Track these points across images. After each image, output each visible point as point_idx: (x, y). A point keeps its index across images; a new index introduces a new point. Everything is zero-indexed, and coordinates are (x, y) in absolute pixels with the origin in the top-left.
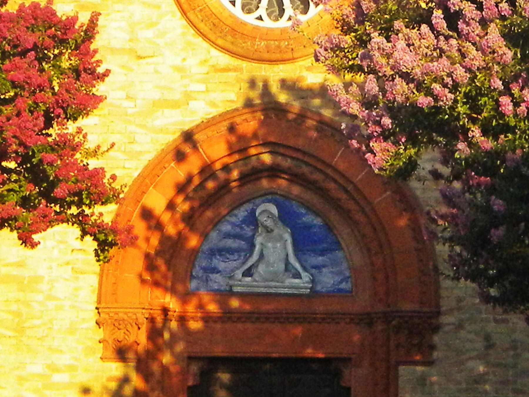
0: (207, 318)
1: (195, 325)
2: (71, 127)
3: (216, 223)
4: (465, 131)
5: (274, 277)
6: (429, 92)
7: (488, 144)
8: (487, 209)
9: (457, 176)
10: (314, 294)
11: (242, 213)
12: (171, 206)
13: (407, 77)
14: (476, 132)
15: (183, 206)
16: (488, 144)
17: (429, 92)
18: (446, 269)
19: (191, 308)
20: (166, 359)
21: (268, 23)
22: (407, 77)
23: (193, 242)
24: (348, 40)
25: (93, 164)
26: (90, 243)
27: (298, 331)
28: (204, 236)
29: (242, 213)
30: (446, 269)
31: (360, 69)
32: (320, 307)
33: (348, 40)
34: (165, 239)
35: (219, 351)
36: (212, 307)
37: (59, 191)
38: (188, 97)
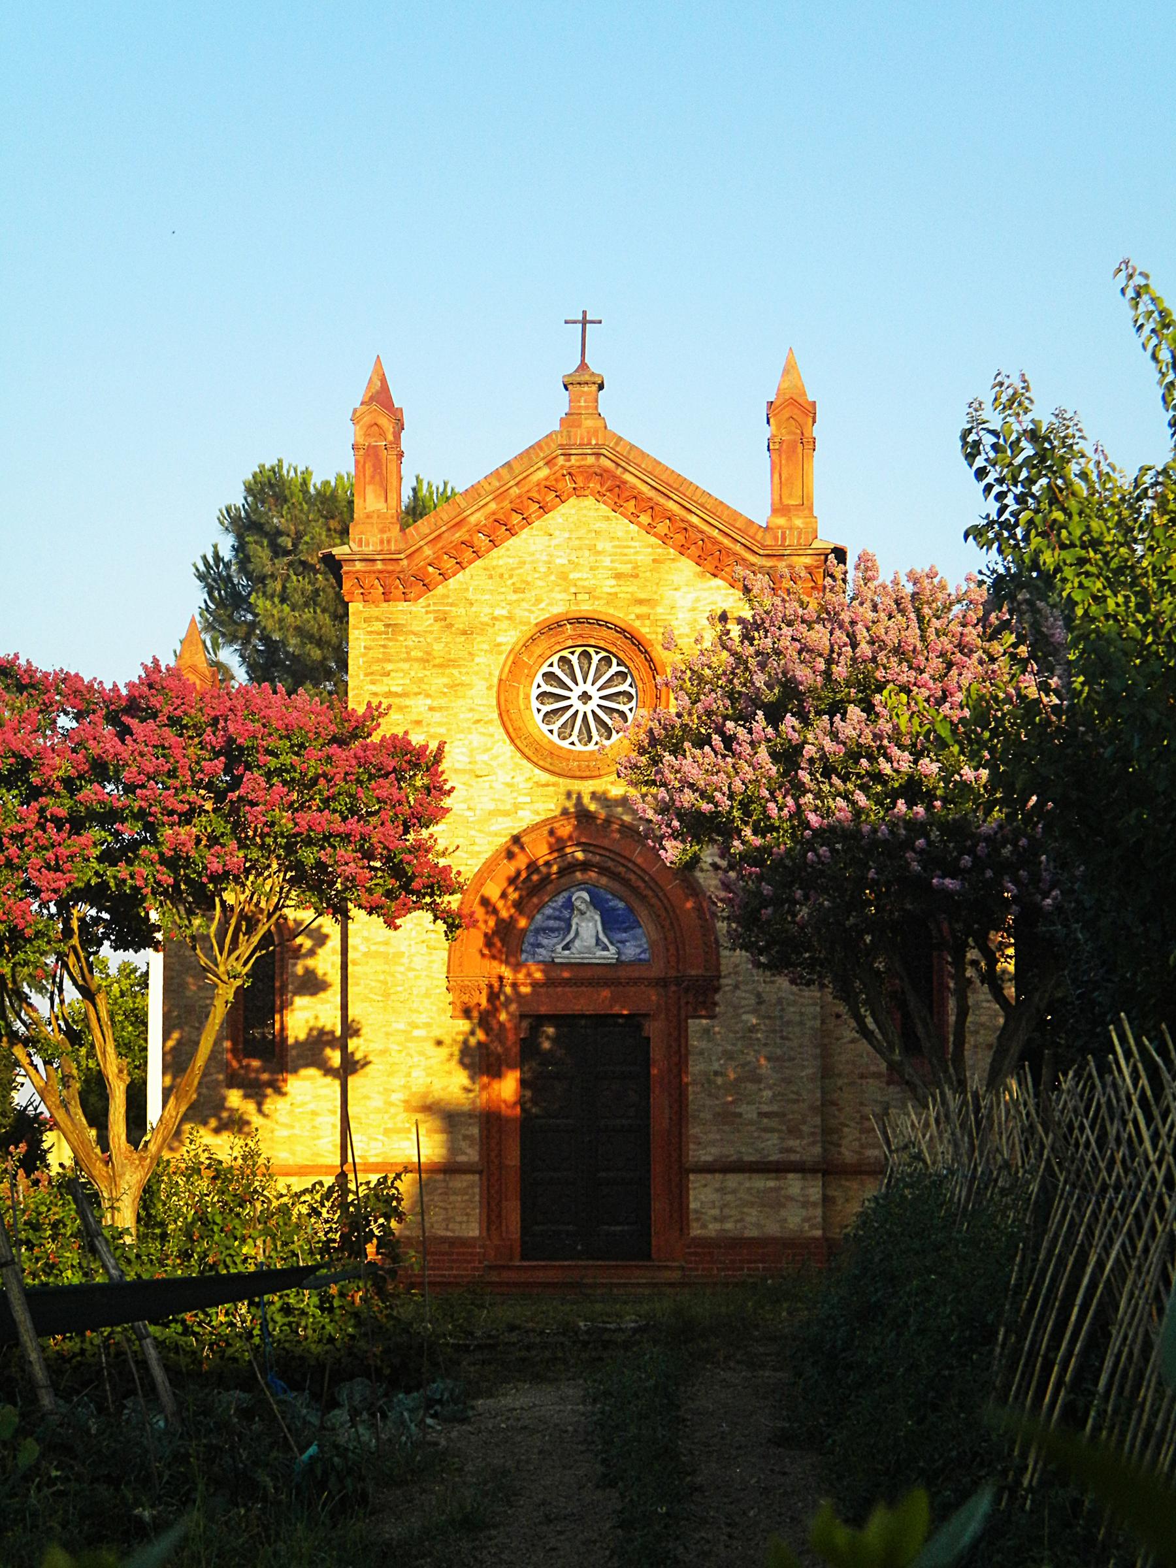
0: (535, 984)
1: (525, 990)
2: (425, 833)
3: (540, 908)
4: (739, 831)
5: (588, 949)
6: (711, 800)
7: (758, 841)
8: (758, 893)
9: (731, 867)
10: (620, 963)
11: (561, 900)
12: (504, 895)
13: (691, 786)
14: (747, 832)
15: (514, 895)
16: (758, 841)
17: (711, 800)
18: (725, 941)
19: (521, 976)
20: (503, 1017)
21: (579, 747)
22: (691, 786)
23: (523, 923)
24: (644, 759)
25: (442, 862)
26: (441, 926)
27: (606, 993)
28: (531, 918)
29: (561, 900)
30: (725, 941)
31: (654, 783)
32: (622, 973)
33: (644, 759)
34: (500, 922)
35: (543, 1010)
36: (538, 975)
37: (415, 885)
38: (517, 807)
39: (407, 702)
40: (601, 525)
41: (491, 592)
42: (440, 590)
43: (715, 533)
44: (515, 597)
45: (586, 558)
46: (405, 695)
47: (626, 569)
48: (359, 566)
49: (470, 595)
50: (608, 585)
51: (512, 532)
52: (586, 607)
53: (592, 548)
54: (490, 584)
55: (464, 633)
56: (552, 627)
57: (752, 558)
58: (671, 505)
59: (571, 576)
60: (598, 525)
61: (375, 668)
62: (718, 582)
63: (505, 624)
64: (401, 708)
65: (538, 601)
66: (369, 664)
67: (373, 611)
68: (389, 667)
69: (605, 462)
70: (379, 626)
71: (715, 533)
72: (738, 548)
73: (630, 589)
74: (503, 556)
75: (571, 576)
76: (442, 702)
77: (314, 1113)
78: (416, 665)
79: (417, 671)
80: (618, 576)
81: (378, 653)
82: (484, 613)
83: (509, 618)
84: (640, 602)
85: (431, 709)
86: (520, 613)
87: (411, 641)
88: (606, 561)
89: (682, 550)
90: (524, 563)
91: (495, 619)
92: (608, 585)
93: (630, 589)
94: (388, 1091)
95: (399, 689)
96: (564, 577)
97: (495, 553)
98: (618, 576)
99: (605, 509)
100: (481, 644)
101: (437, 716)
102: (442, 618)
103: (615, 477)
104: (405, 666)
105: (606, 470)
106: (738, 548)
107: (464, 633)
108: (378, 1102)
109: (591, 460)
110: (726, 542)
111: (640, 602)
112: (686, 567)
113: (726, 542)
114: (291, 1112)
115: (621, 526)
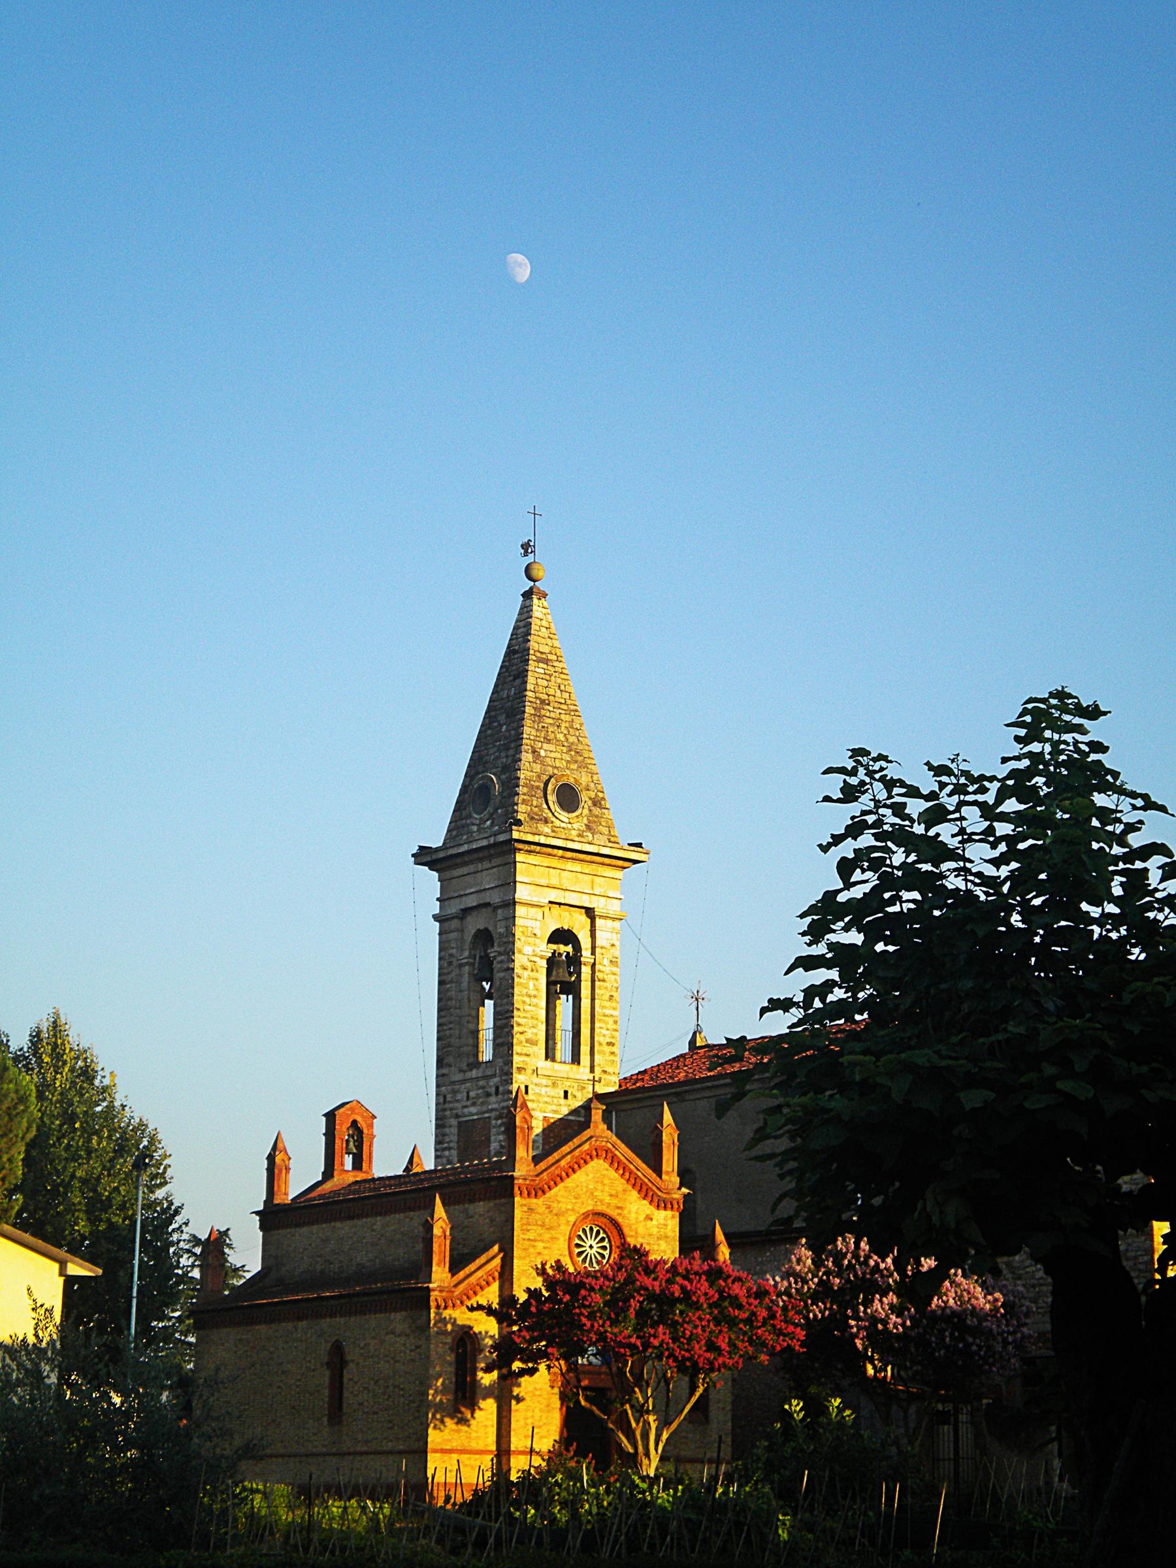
39: (536, 1244)
40: (605, 1172)
41: (567, 1197)
42: (548, 1195)
43: (646, 1180)
44: (574, 1201)
45: (599, 1186)
46: (535, 1240)
47: (614, 1192)
48: (520, 1181)
49: (558, 1198)
50: (607, 1199)
51: (574, 1171)
52: (600, 1208)
53: (602, 1182)
54: (565, 1194)
55: (556, 1215)
56: (586, 1215)
57: (660, 1193)
58: (632, 1167)
59: (596, 1194)
60: (605, 1172)
61: (524, 1227)
62: (645, 1202)
63: (571, 1213)
64: (534, 1246)
65: (583, 1203)
66: (523, 1225)
67: (524, 1202)
68: (529, 1227)
69: (609, 1146)
70: (525, 1209)
71: (646, 1180)
72: (654, 1188)
73: (615, 1202)
74: (569, 1182)
75: (596, 1194)
76: (548, 1245)
77: (486, 1426)
78: (540, 1228)
79: (540, 1230)
80: (611, 1195)
81: (524, 1221)
82: (563, 1206)
83: (573, 1210)
84: (618, 1208)
85: (544, 1248)
86: (576, 1208)
87: (538, 1217)
88: (607, 1189)
89: (634, 1186)
90: (577, 1186)
91: (568, 1210)
92: (607, 1199)
93: (615, 1202)
94: (526, 1418)
95: (532, 1238)
96: (592, 1194)
97: (568, 1180)
98: (611, 1195)
99: (606, 1165)
100: (563, 1220)
101: (546, 1252)
102: (549, 1207)
103: (612, 1152)
104: (535, 1228)
105: (609, 1149)
106: (654, 1188)
107: (556, 1215)
108: (522, 1423)
109: (604, 1143)
110: (650, 1184)
111: (618, 1208)
112: (634, 1194)
113: (650, 1184)
114: (477, 1426)
115: (612, 1173)
